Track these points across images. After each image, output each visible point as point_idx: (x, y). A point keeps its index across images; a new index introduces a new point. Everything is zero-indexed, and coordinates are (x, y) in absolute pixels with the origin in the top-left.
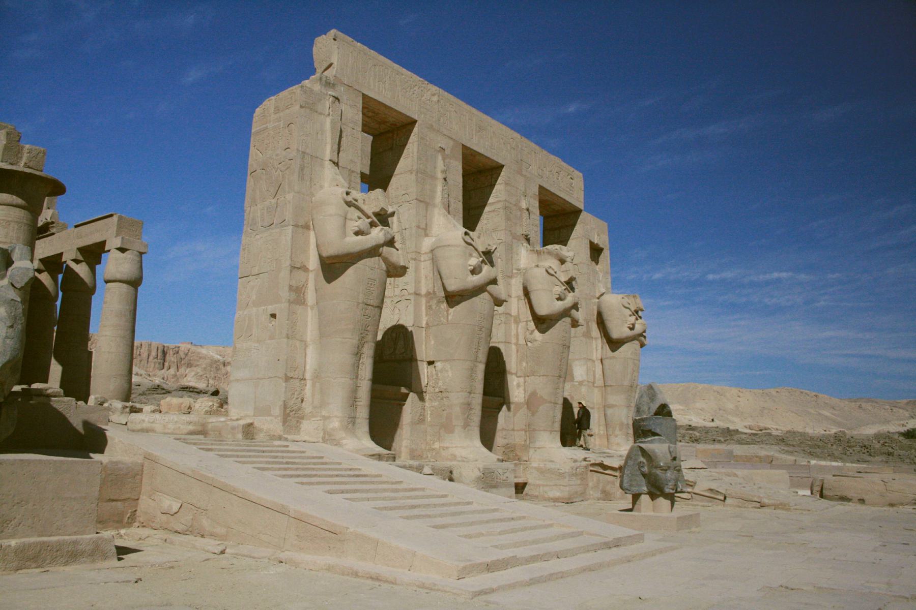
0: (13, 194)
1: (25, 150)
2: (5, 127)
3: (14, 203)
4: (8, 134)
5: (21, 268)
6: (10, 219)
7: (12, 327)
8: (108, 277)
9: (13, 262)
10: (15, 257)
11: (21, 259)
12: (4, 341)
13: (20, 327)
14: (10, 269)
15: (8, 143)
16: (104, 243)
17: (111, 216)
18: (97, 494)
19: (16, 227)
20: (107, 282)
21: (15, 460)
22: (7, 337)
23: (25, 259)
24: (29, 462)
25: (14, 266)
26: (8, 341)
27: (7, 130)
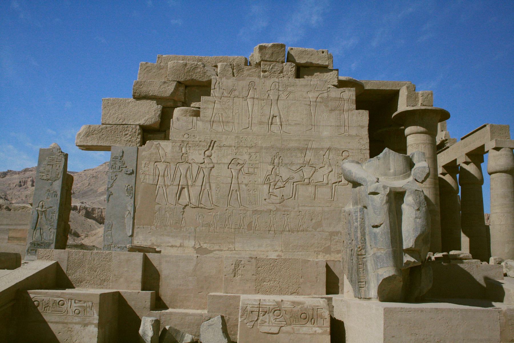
0: (417, 126)
1: (420, 95)
2: (405, 84)
3: (419, 131)
4: (408, 88)
5: (420, 167)
6: (418, 142)
7: (418, 210)
8: (491, 170)
9: (414, 164)
10: (415, 161)
11: (419, 162)
12: (415, 221)
13: (424, 209)
14: (413, 169)
15: (408, 93)
16: (483, 147)
17: (485, 126)
18: (498, 337)
19: (423, 146)
20: (490, 174)
21: (432, 309)
22: (416, 218)
23: (422, 161)
24: (442, 310)
25: (415, 167)
26: (418, 220)
27: (406, 85)
